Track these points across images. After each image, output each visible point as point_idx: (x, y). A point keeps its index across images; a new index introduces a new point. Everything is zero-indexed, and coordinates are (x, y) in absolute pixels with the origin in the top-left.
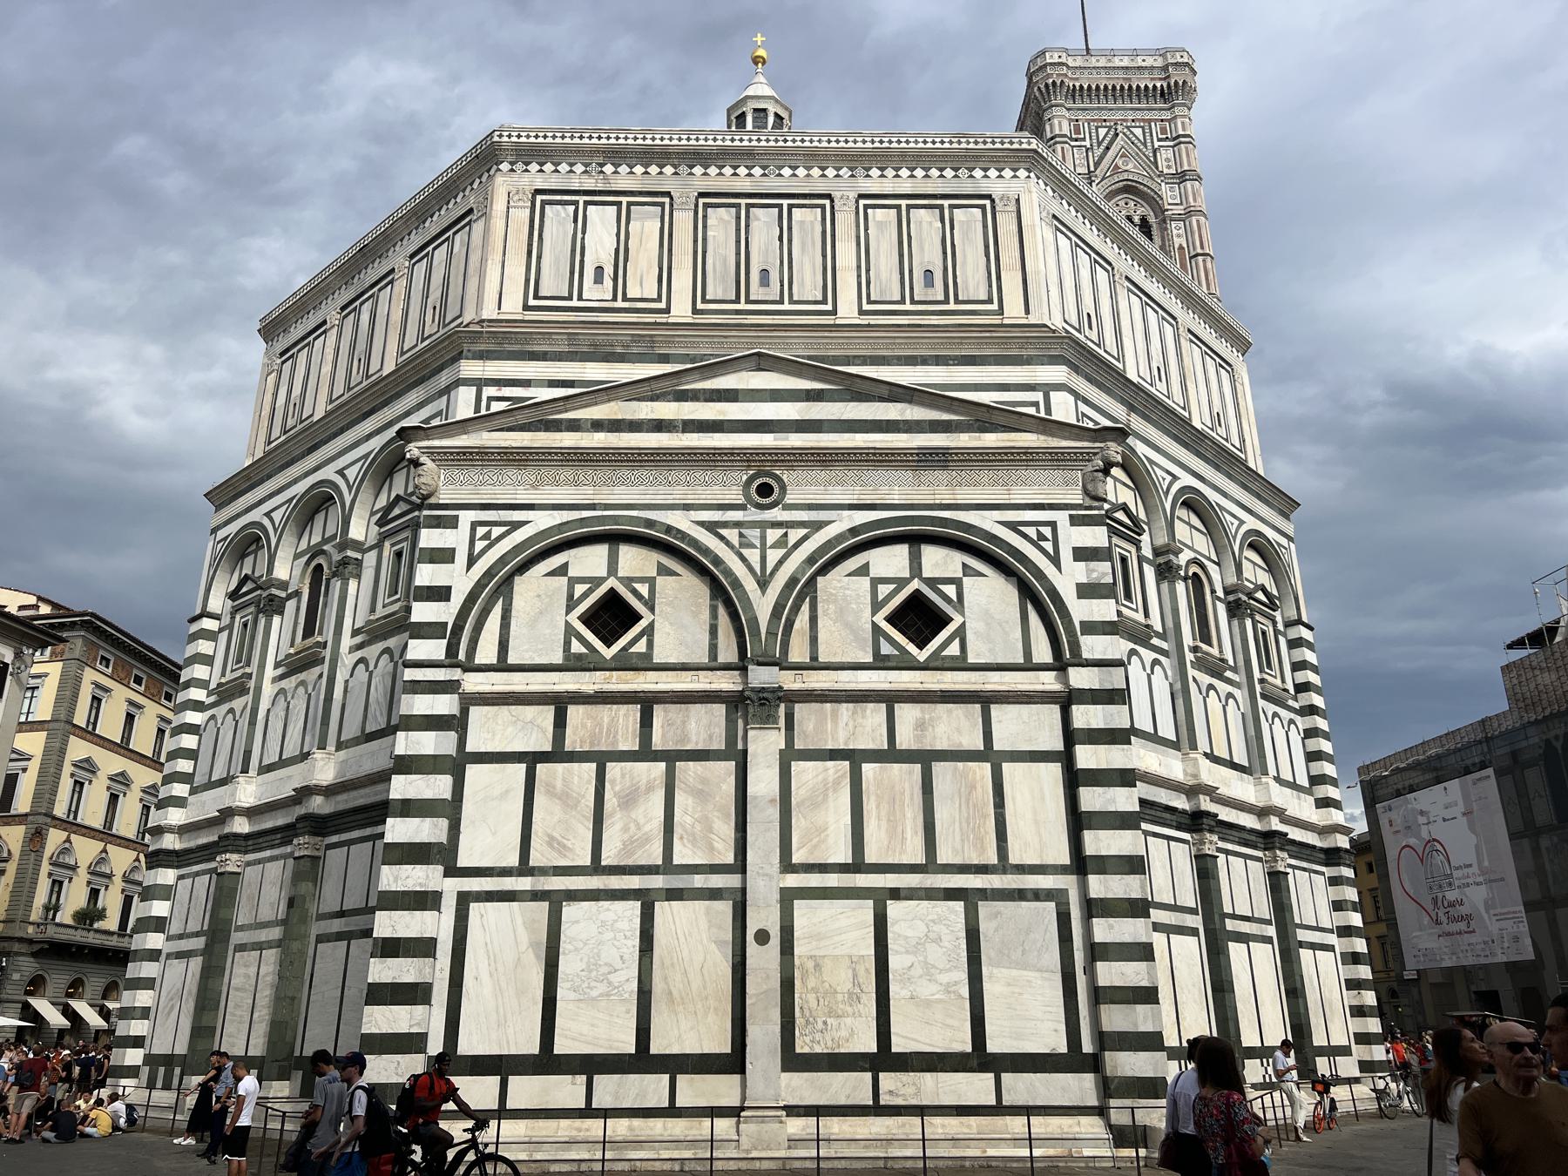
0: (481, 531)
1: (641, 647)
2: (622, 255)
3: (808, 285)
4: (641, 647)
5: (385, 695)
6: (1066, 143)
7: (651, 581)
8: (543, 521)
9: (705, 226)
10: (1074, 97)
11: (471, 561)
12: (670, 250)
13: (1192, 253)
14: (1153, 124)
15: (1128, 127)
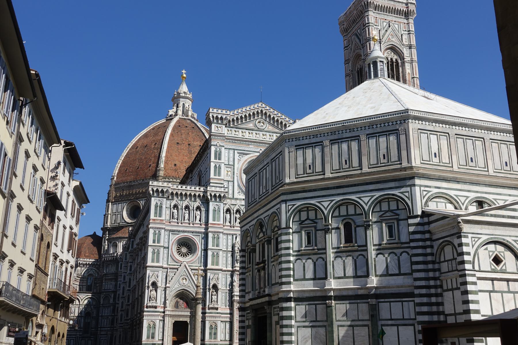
0: (473, 239)
1: (504, 268)
2: (439, 149)
3: (481, 163)
4: (504, 268)
5: (396, 264)
6: (373, 26)
7: (503, 252)
8: (484, 238)
9: (457, 144)
10: (376, 8)
11: (473, 246)
12: (451, 150)
13: (413, 77)
14: (401, 24)
15: (393, 24)
